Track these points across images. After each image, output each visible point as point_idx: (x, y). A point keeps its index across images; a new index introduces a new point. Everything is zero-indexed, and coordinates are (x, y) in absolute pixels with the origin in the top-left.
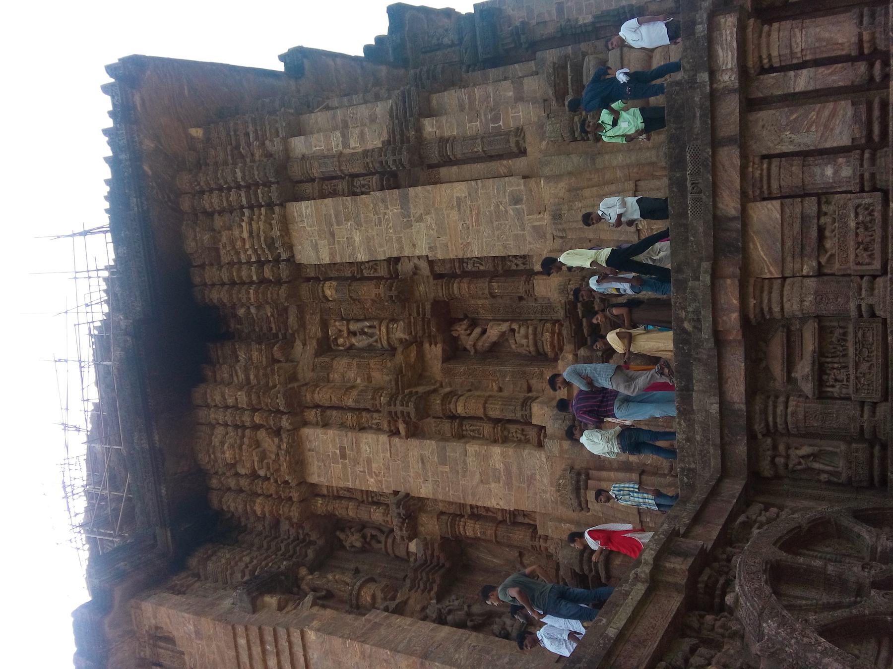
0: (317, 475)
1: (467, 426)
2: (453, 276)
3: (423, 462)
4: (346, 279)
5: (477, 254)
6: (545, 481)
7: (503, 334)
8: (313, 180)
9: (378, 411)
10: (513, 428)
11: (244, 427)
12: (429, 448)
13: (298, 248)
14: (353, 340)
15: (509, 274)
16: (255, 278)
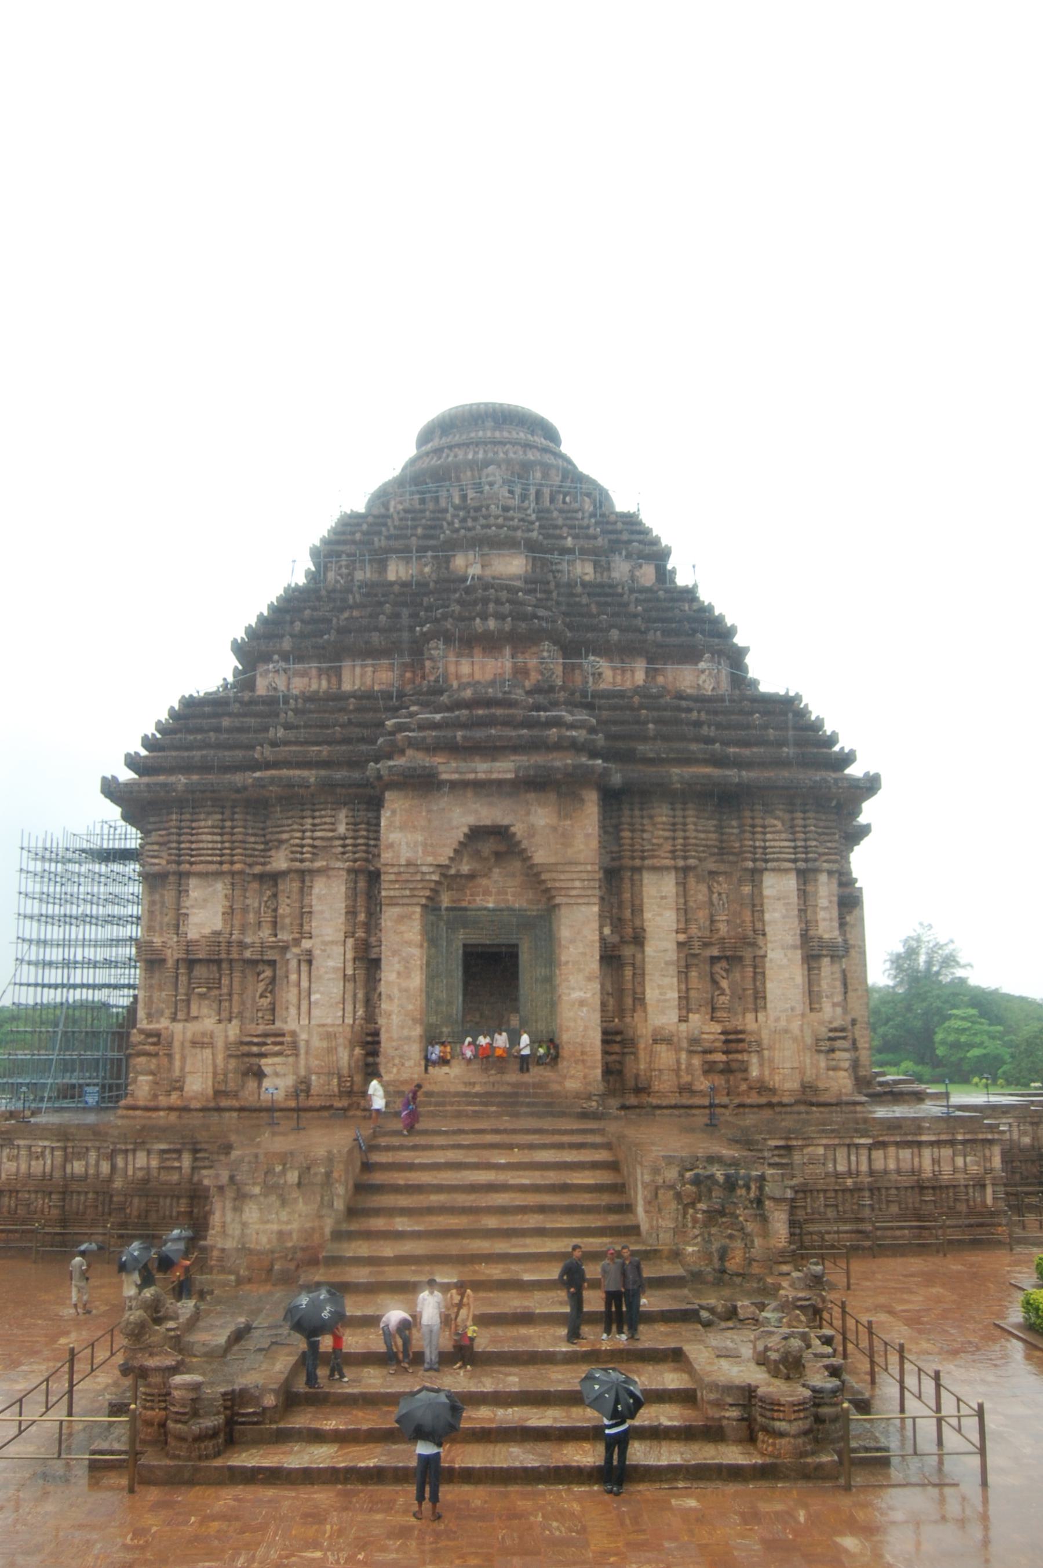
0: (648, 878)
1: (683, 976)
2: (755, 967)
3: (665, 951)
4: (753, 899)
5: (769, 985)
6: (664, 1021)
7: (723, 990)
8: (805, 884)
9: (687, 921)
10: (684, 1002)
11: (674, 831)
12: (672, 955)
13: (772, 874)
14: (715, 896)
15: (756, 998)
16: (757, 844)
